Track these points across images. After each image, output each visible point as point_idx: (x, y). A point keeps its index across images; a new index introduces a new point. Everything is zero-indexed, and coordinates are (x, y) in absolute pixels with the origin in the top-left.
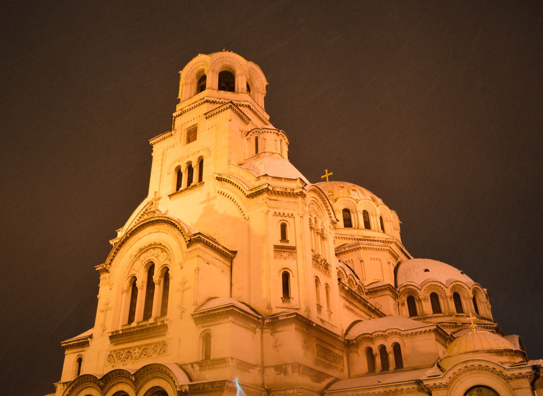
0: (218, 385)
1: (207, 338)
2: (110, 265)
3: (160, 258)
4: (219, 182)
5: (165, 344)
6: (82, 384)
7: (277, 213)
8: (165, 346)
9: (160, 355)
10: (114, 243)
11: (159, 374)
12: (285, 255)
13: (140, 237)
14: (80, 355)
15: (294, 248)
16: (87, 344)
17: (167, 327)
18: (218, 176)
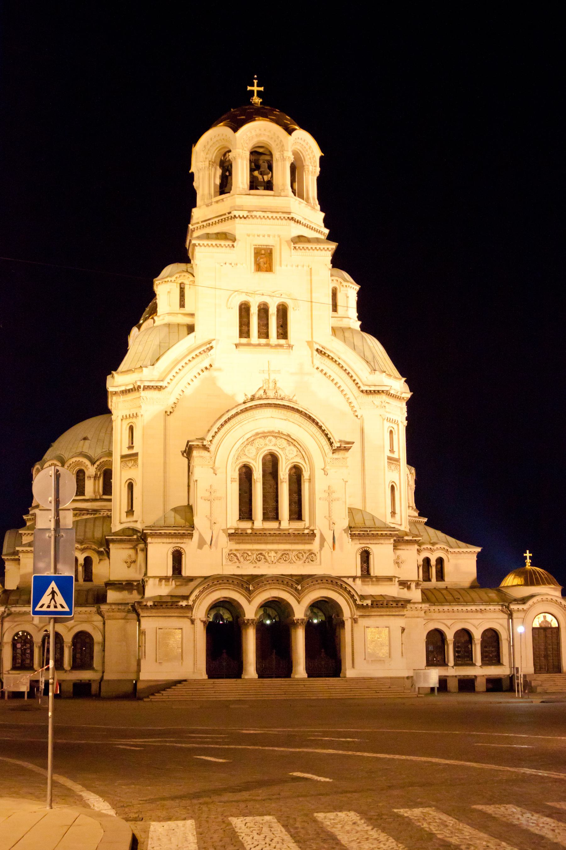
0: (403, 603)
1: (366, 556)
2: (211, 443)
3: (287, 451)
4: (318, 355)
5: (313, 553)
6: (215, 585)
7: (389, 419)
8: (313, 555)
9: (306, 563)
10: (144, 386)
11: (330, 586)
12: (393, 467)
13: (256, 418)
14: (177, 547)
15: (397, 460)
16: (190, 536)
17: (315, 536)
18: (321, 349)
